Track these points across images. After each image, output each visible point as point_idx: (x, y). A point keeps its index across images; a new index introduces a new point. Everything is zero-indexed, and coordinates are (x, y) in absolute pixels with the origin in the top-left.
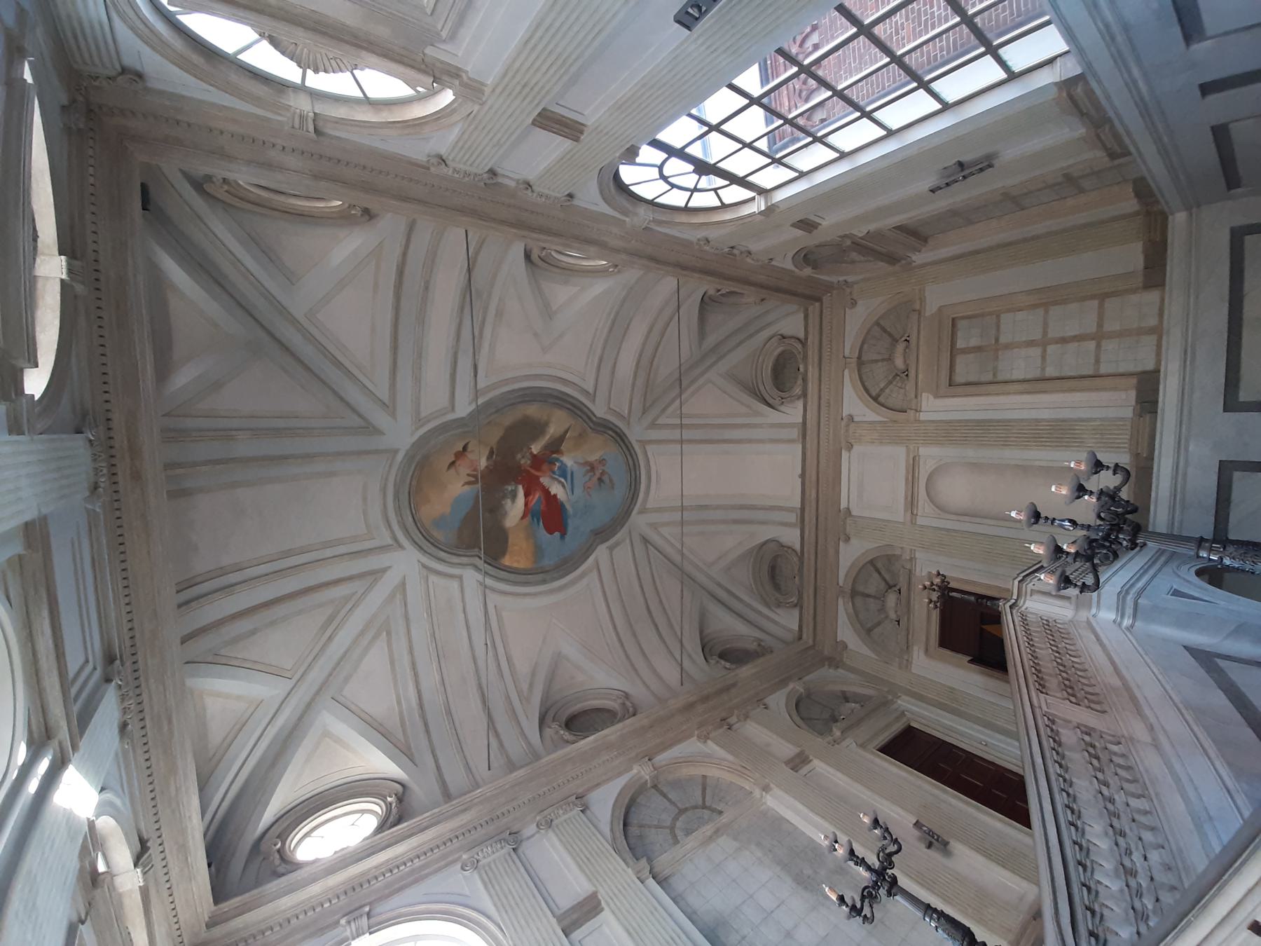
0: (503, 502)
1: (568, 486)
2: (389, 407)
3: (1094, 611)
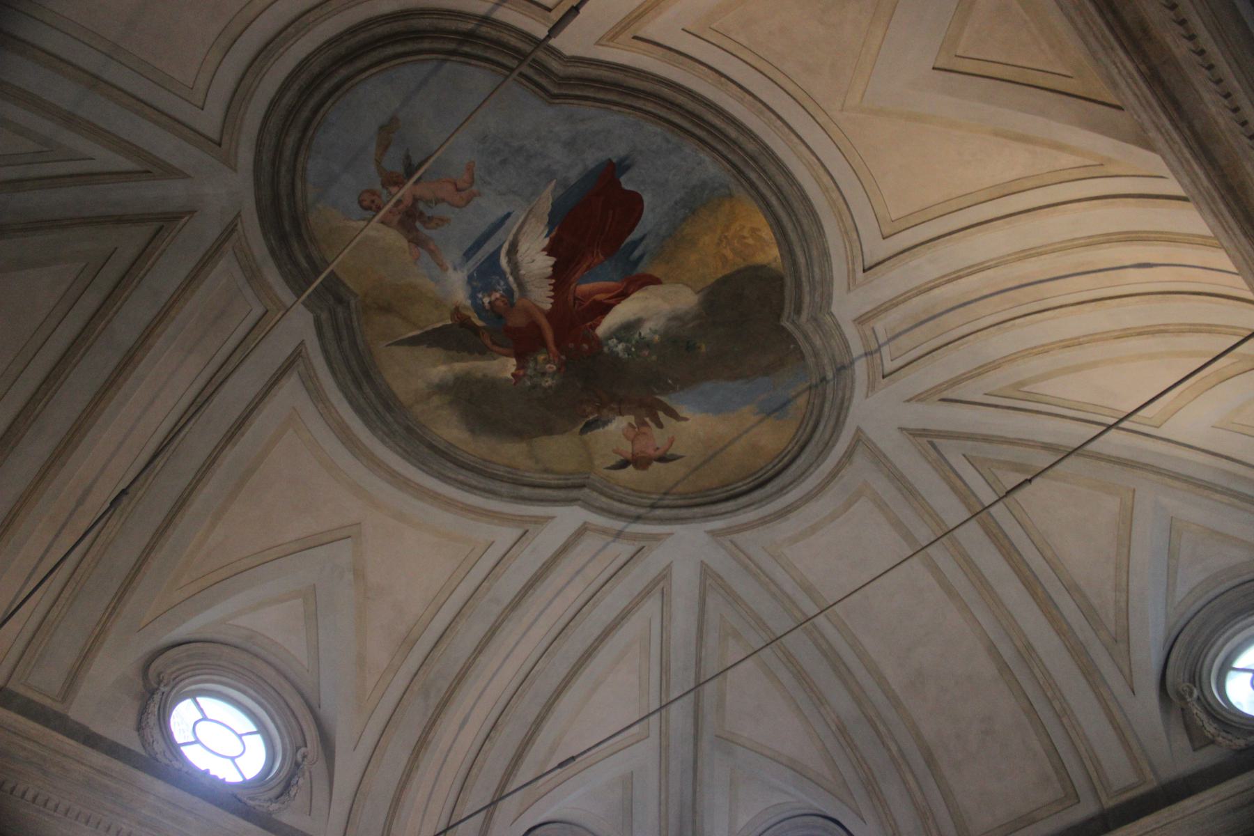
0: (657, 337)
1: (504, 238)
2: (660, 584)
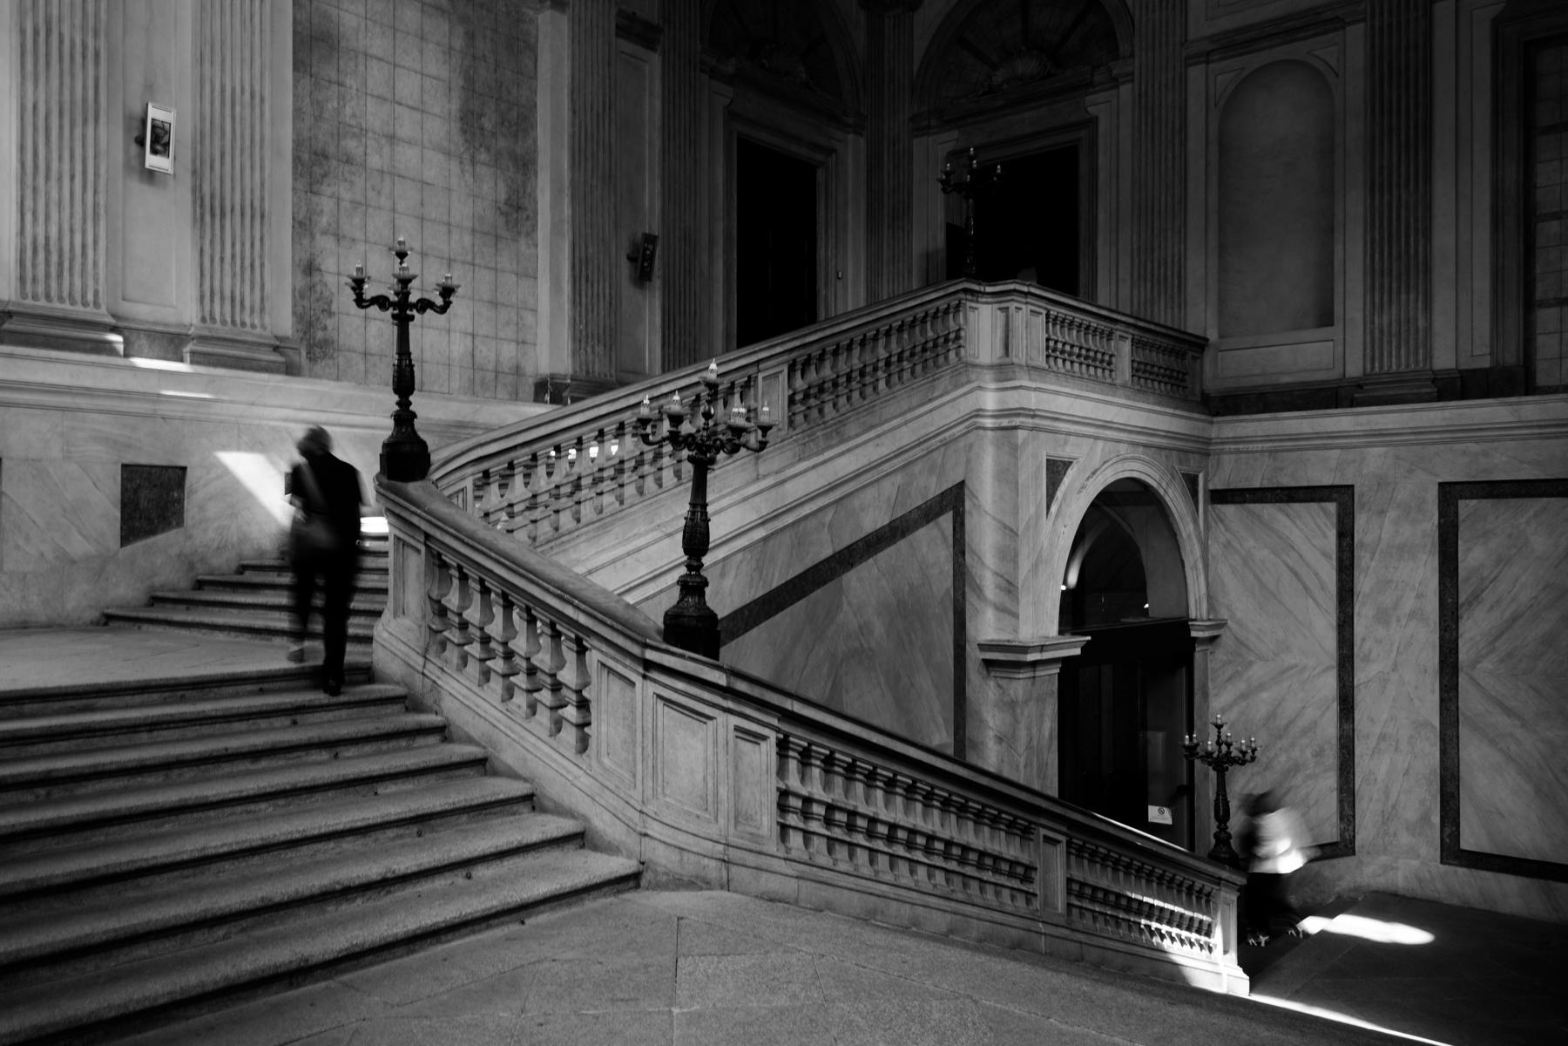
3: (993, 386)
